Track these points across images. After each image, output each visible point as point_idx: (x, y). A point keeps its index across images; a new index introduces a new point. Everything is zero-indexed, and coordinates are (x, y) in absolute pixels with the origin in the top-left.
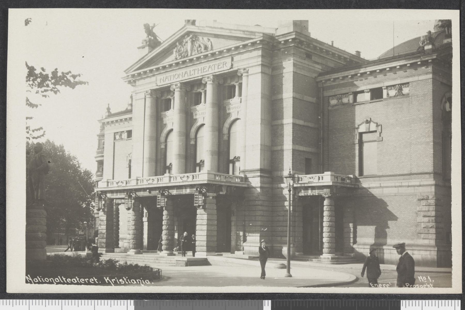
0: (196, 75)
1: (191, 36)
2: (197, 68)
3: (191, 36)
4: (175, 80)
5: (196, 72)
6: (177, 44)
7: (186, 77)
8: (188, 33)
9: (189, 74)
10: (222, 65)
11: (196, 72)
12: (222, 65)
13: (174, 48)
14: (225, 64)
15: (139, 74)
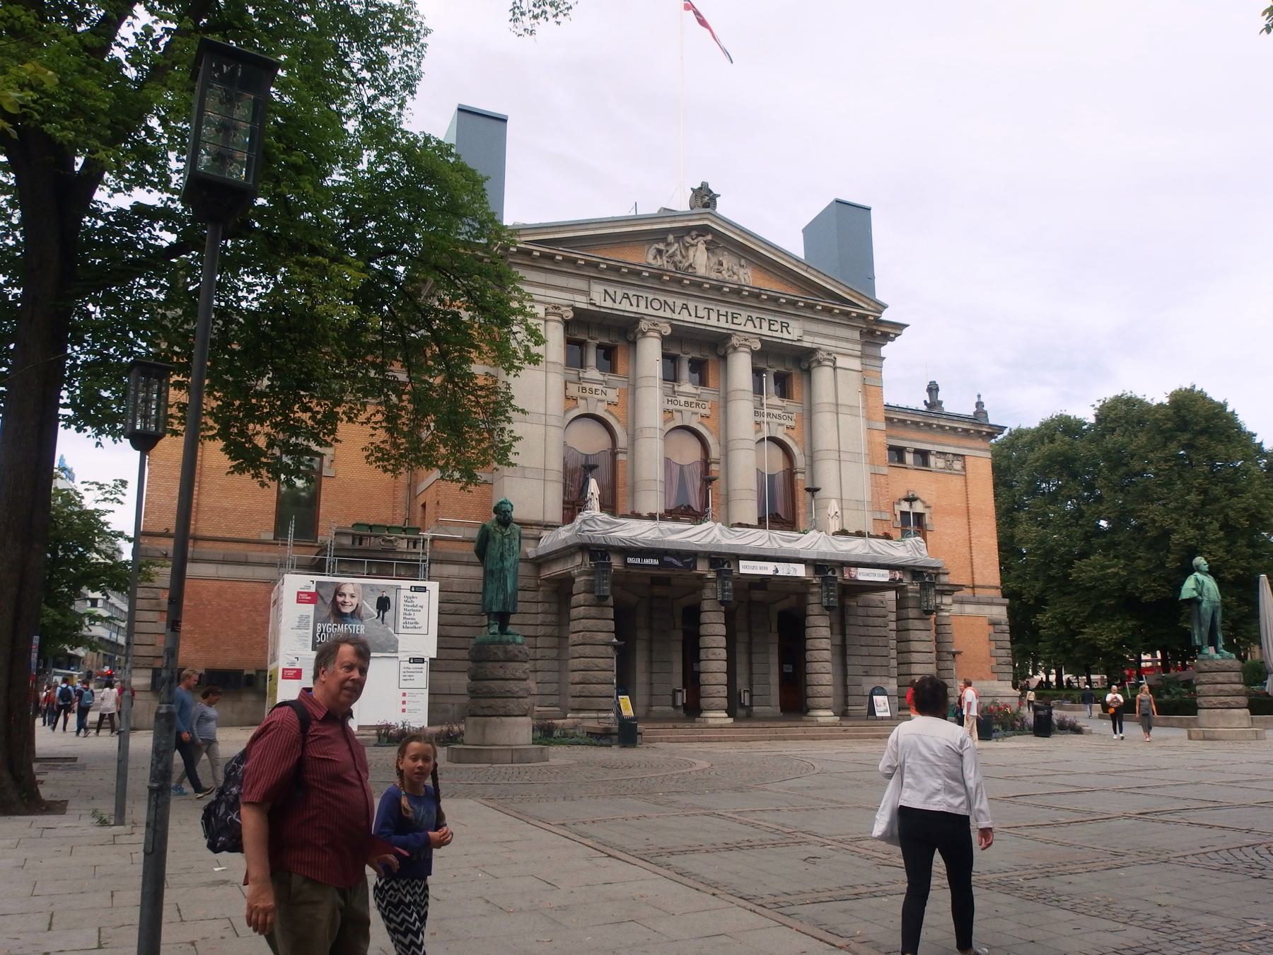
0: (713, 321)
1: (709, 237)
2: (715, 308)
3: (709, 237)
4: (650, 311)
5: (714, 316)
6: (671, 238)
7: (684, 316)
8: (704, 230)
9: (693, 314)
10: (777, 327)
11: (714, 316)
12: (777, 327)
13: (657, 241)
14: (785, 326)
15: (543, 255)
